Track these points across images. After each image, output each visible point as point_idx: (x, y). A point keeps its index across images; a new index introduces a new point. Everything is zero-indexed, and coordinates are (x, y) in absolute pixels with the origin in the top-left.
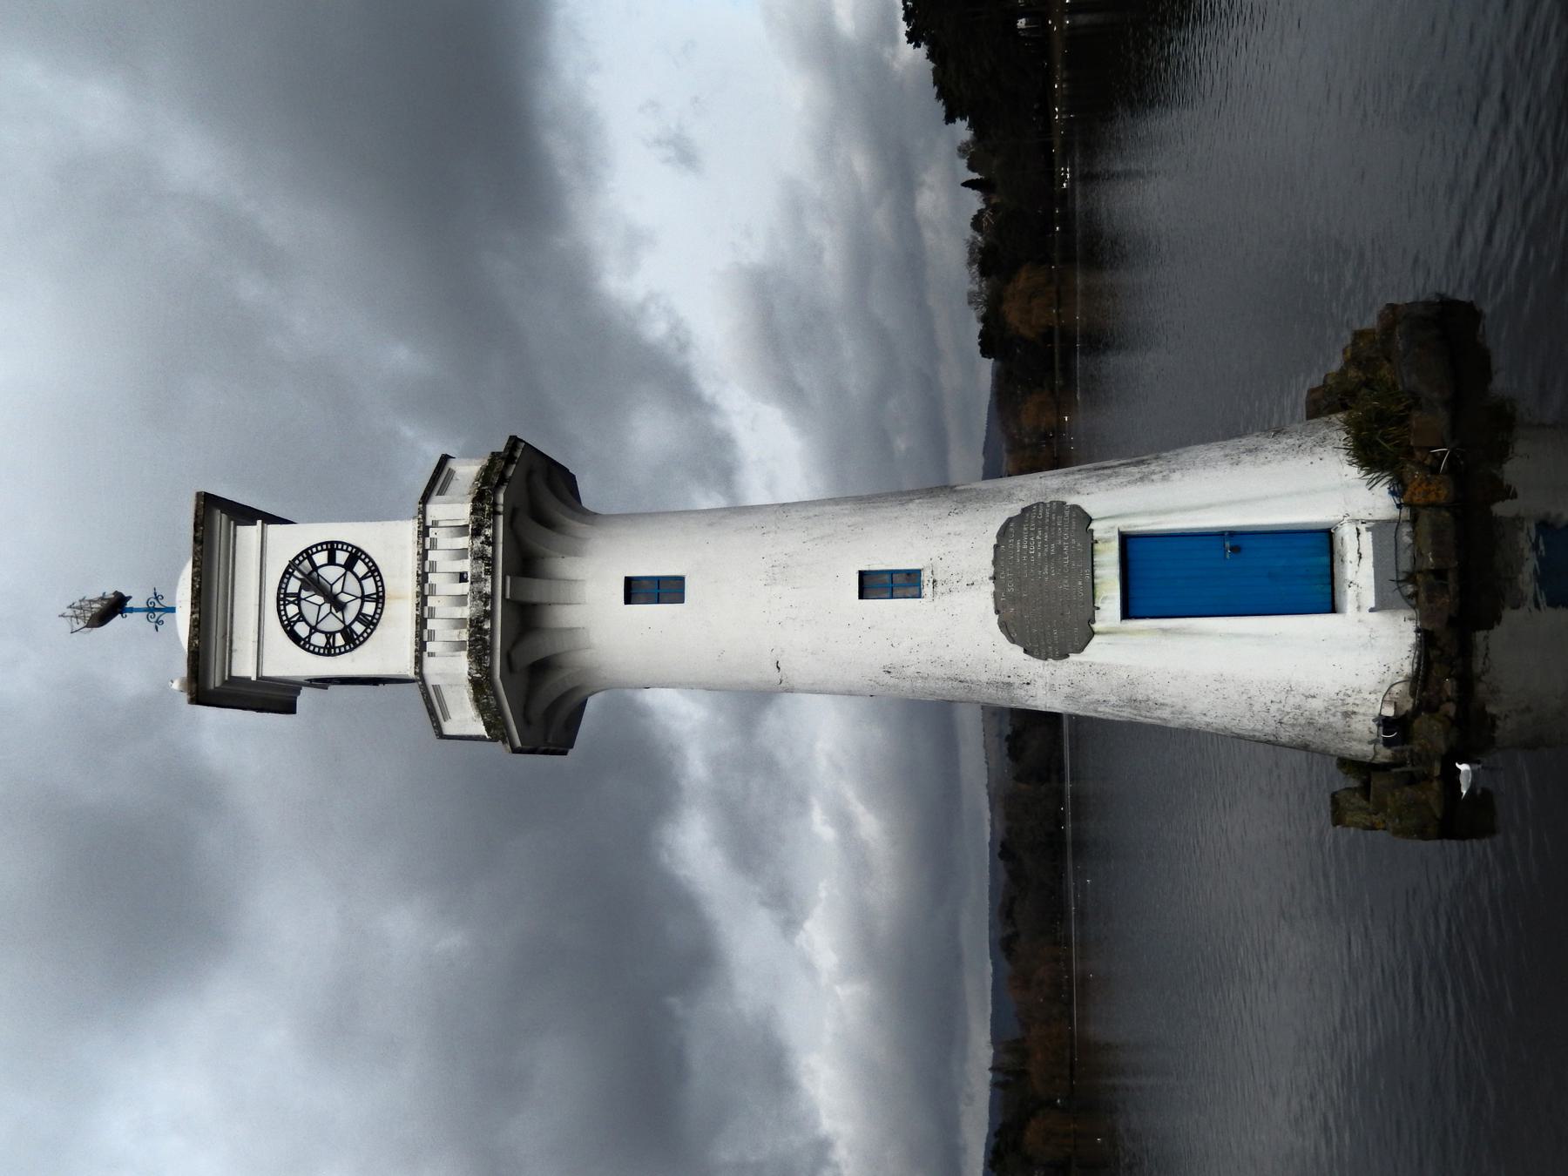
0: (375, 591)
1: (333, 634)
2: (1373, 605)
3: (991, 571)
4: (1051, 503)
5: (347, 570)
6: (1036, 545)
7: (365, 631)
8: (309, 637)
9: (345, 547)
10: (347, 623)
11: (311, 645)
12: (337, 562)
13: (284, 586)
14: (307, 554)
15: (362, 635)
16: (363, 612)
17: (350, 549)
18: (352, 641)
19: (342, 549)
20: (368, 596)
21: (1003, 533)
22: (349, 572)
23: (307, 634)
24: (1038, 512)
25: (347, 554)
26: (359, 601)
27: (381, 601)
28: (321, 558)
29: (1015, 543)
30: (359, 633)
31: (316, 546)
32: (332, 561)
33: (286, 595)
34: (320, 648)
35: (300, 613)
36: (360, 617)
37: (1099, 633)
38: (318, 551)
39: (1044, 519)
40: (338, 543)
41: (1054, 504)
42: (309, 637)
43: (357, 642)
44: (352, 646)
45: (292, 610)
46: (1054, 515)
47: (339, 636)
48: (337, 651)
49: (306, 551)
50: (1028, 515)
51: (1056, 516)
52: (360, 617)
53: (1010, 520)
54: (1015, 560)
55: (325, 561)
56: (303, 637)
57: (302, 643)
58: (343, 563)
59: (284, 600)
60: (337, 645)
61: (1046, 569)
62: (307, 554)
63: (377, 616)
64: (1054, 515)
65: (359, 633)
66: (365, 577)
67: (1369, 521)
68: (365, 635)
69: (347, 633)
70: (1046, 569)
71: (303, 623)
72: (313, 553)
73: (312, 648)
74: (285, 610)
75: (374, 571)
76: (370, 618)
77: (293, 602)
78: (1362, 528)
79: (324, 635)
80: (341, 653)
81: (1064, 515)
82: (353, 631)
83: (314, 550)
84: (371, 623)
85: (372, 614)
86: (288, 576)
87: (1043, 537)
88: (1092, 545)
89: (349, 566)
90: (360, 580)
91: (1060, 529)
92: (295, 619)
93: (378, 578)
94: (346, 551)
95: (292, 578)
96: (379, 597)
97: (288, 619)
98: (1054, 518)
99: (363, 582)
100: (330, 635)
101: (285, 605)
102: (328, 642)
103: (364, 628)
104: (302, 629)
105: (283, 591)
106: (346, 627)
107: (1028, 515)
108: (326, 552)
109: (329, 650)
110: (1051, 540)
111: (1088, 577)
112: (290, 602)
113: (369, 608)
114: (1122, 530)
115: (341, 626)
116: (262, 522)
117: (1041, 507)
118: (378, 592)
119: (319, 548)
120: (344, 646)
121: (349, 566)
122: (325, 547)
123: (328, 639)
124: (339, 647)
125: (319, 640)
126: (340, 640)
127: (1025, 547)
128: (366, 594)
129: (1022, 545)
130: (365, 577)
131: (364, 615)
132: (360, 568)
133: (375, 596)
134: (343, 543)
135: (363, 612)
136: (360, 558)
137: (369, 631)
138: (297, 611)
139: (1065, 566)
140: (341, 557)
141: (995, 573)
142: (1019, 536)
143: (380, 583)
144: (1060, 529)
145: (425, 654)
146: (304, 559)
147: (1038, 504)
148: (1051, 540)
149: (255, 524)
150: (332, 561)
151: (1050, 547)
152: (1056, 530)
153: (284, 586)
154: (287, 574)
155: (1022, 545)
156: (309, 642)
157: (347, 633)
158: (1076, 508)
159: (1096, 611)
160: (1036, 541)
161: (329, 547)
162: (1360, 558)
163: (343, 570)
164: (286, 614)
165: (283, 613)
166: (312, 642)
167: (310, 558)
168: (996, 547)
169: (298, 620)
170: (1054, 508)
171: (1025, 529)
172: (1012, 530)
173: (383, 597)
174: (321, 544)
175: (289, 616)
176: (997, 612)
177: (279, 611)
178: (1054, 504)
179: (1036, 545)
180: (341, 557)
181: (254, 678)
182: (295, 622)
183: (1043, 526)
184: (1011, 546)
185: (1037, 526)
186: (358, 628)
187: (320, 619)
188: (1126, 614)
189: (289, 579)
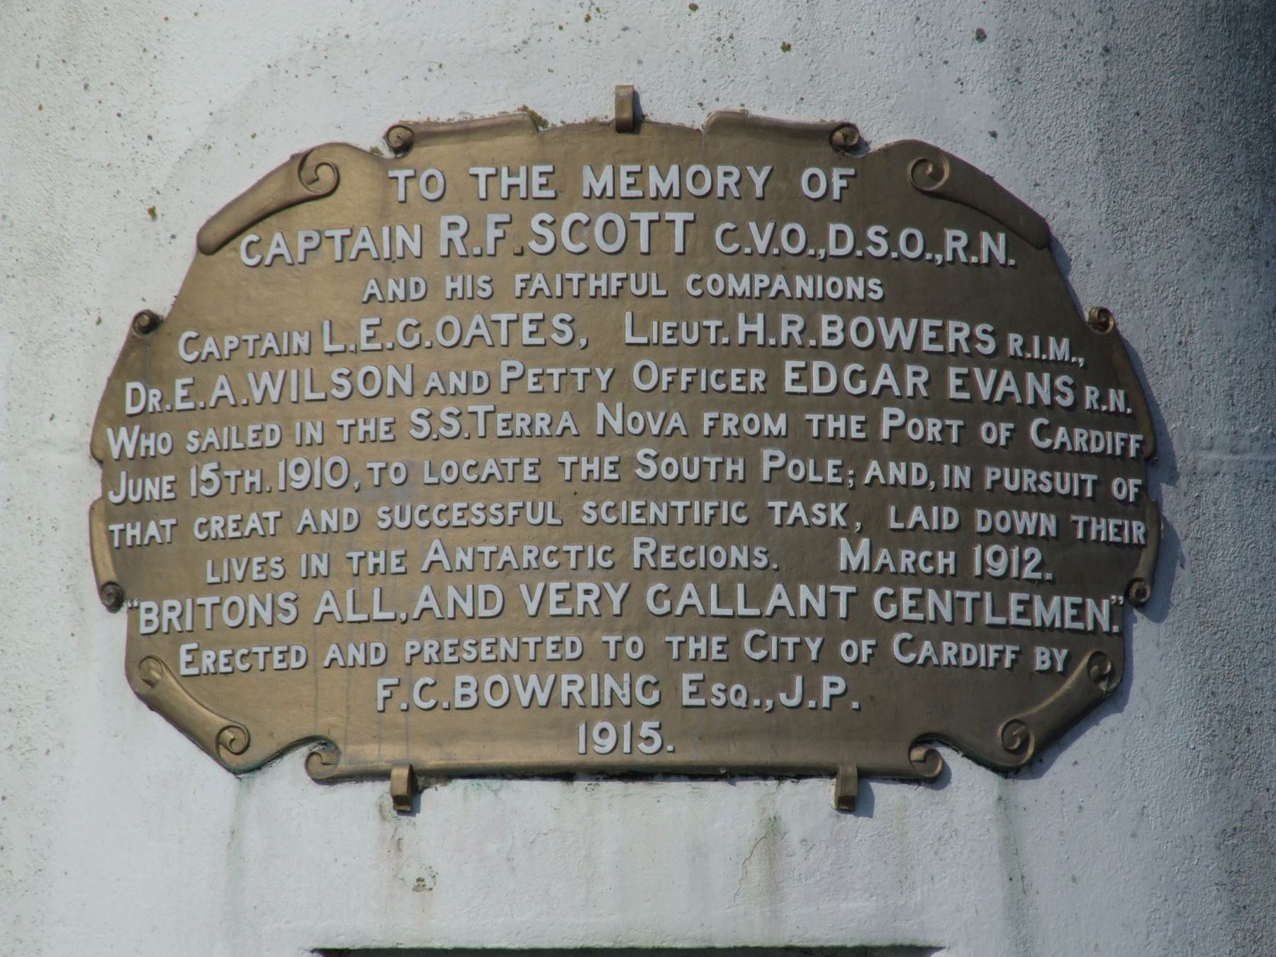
6: (838, 401)
24: (1075, 416)
29: (860, 264)
41: (1137, 530)
46: (1049, 524)
50: (1059, 349)
51: (1034, 539)
61: (671, 465)
87: (900, 447)
98: (1025, 521)
117: (1111, 442)
127: (830, 329)
129: (848, 307)
144: (946, 561)
151: (825, 492)
152: (938, 538)
155: (848, 307)
160: (871, 404)
171: (957, 333)
172: (955, 240)
178: (1137, 530)
185: (975, 410)
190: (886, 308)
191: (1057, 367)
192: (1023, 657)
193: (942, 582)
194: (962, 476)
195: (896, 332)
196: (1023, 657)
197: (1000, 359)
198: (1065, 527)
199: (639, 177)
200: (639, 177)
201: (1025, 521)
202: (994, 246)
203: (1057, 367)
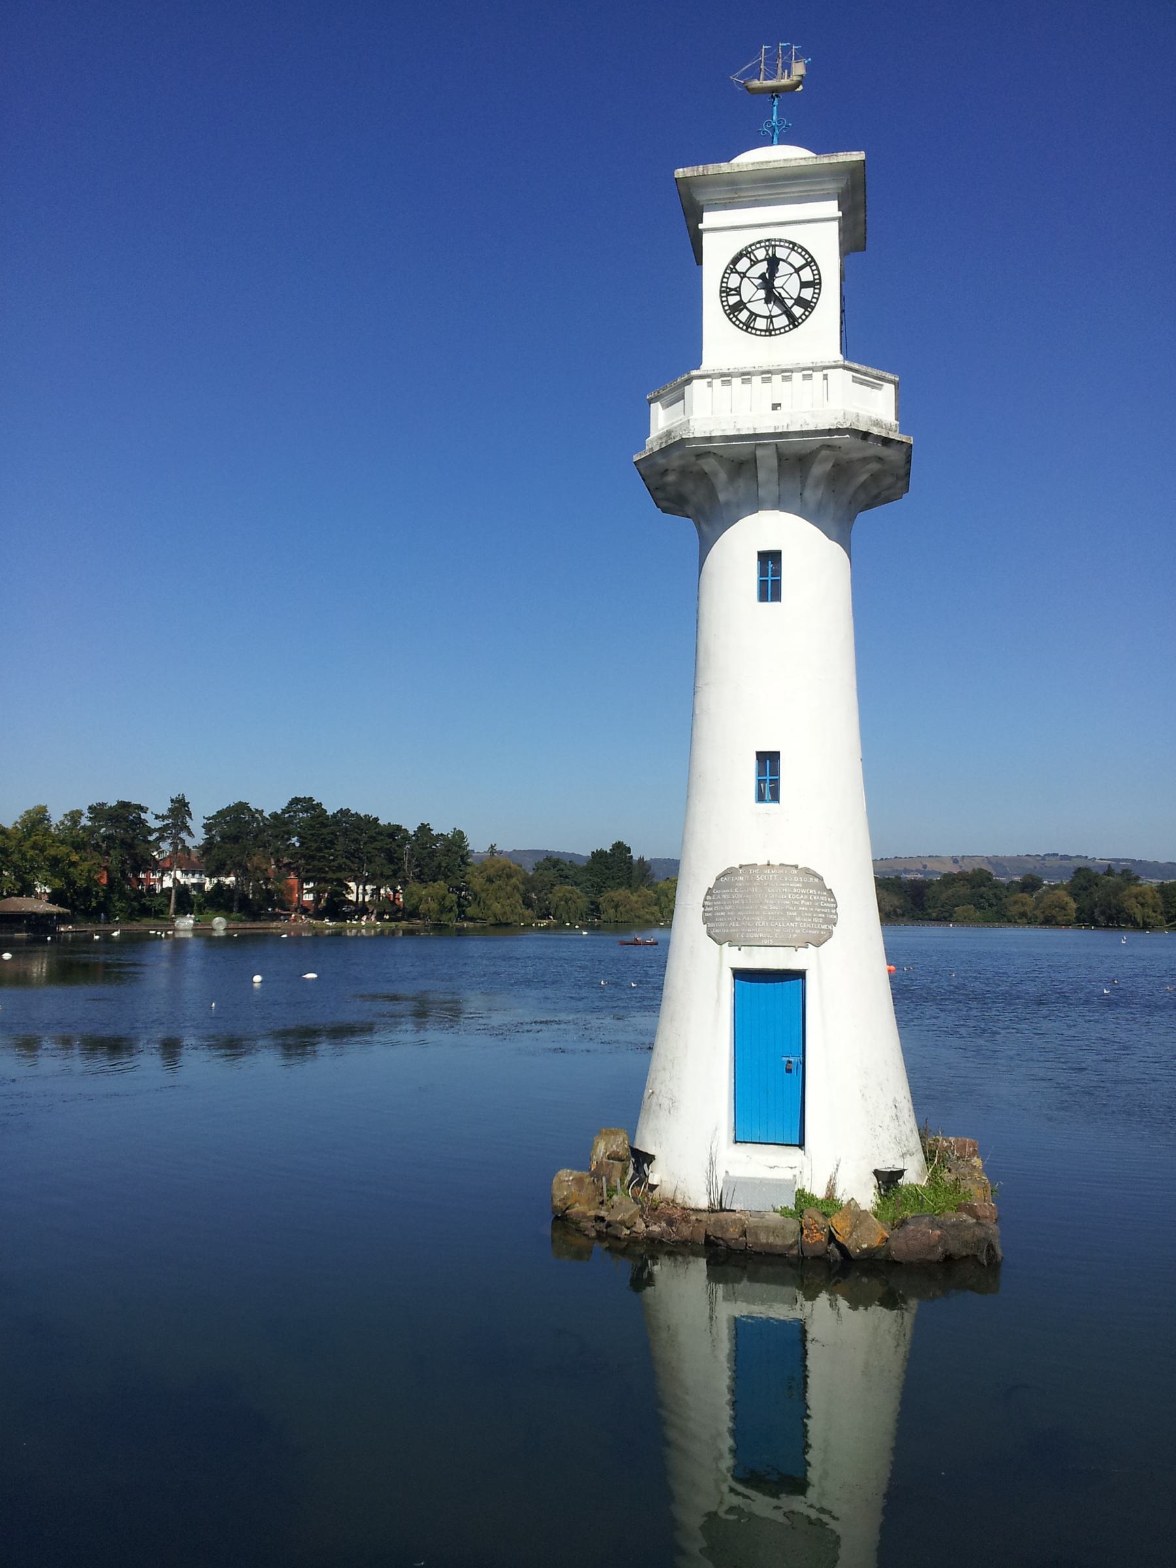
0: (775, 327)
1: (739, 294)
2: (730, 1174)
3: (775, 862)
4: (836, 914)
5: (795, 300)
6: (796, 899)
7: (741, 322)
8: (737, 272)
9: (816, 296)
10: (748, 305)
11: (730, 274)
12: (802, 290)
13: (782, 244)
14: (811, 262)
15: (738, 319)
16: (758, 318)
17: (814, 300)
18: (733, 311)
19: (814, 293)
20: (772, 322)
21: (808, 872)
22: (793, 301)
24: (827, 902)
25: (809, 299)
26: (767, 314)
27: (767, 334)
28: (807, 275)
31: (818, 269)
34: (727, 283)
36: (753, 316)
37: (721, 949)
38: (813, 271)
39: (820, 907)
41: (835, 917)
42: (737, 272)
43: (731, 316)
44: (728, 312)
45: (760, 254)
46: (823, 916)
47: (737, 298)
48: (724, 299)
49: (813, 260)
50: (825, 893)
51: (822, 918)
53: (821, 879)
54: (784, 882)
56: (736, 267)
57: (732, 266)
58: (801, 295)
60: (729, 297)
61: (774, 908)
62: (811, 262)
63: (754, 331)
64: (823, 916)
67: (802, 1178)
68: (737, 323)
69: (740, 306)
70: (774, 908)
71: (749, 265)
72: (811, 267)
73: (727, 275)
74: (761, 247)
76: (752, 325)
77: (767, 254)
78: (796, 1172)
79: (738, 285)
80: (722, 302)
81: (823, 924)
82: (741, 311)
83: (814, 268)
84: (748, 327)
85: (755, 327)
86: (791, 246)
87: (804, 905)
88: (794, 947)
91: (810, 920)
92: (753, 257)
93: (787, 329)
94: (813, 297)
95: (789, 251)
97: (753, 250)
98: (820, 915)
100: (738, 291)
101: (765, 247)
102: (731, 290)
103: (744, 321)
104: (743, 264)
105: (777, 243)
106: (745, 304)
107: (825, 893)
108: (812, 279)
109: (725, 291)
110: (800, 913)
111: (766, 942)
112: (767, 251)
113: (761, 324)
114: (807, 972)
115: (745, 301)
116: (839, 219)
117: (832, 905)
118: (775, 330)
119: (816, 272)
120: (728, 305)
122: (817, 277)
123: (735, 290)
124: (727, 301)
125: (734, 280)
126: (733, 300)
127: (795, 890)
128: (774, 319)
131: (755, 320)
133: (771, 328)
135: (758, 318)
136: (806, 310)
137: (741, 325)
138: (759, 259)
139: (776, 924)
141: (773, 866)
142: (806, 885)
144: (810, 920)
145: (710, 380)
146: (806, 260)
147: (835, 902)
148: (800, 913)
149: (839, 210)
150: (804, 285)
151: (794, 911)
152: (809, 917)
153: (782, 244)
154: (793, 246)
155: (797, 888)
156: (732, 272)
157: (740, 306)
158: (830, 934)
159: (737, 947)
160: (800, 900)
161: (816, 281)
162: (771, 1168)
164: (757, 248)
165: (758, 246)
166: (732, 275)
167: (807, 264)
168: (796, 867)
169: (751, 260)
170: (831, 916)
171: (811, 891)
172: (811, 879)
173: (771, 335)
174: (819, 274)
175: (755, 252)
176: (741, 867)
178: (835, 917)
179: (796, 899)
181: (701, 226)
182: (750, 258)
183: (814, 906)
184: (796, 879)
185: (814, 901)
186: (744, 316)
187: (752, 279)
188: (740, 975)
189: (788, 248)
190: (802, 888)
191: (824, 896)
192: (820, 932)
193: (809, 922)
194: (812, 909)
195: (803, 891)
196: (820, 932)
197: (817, 895)
198: (826, 916)
199: (770, 871)
200: (770, 871)
201: (820, 915)
202: (816, 880)
203: (824, 896)
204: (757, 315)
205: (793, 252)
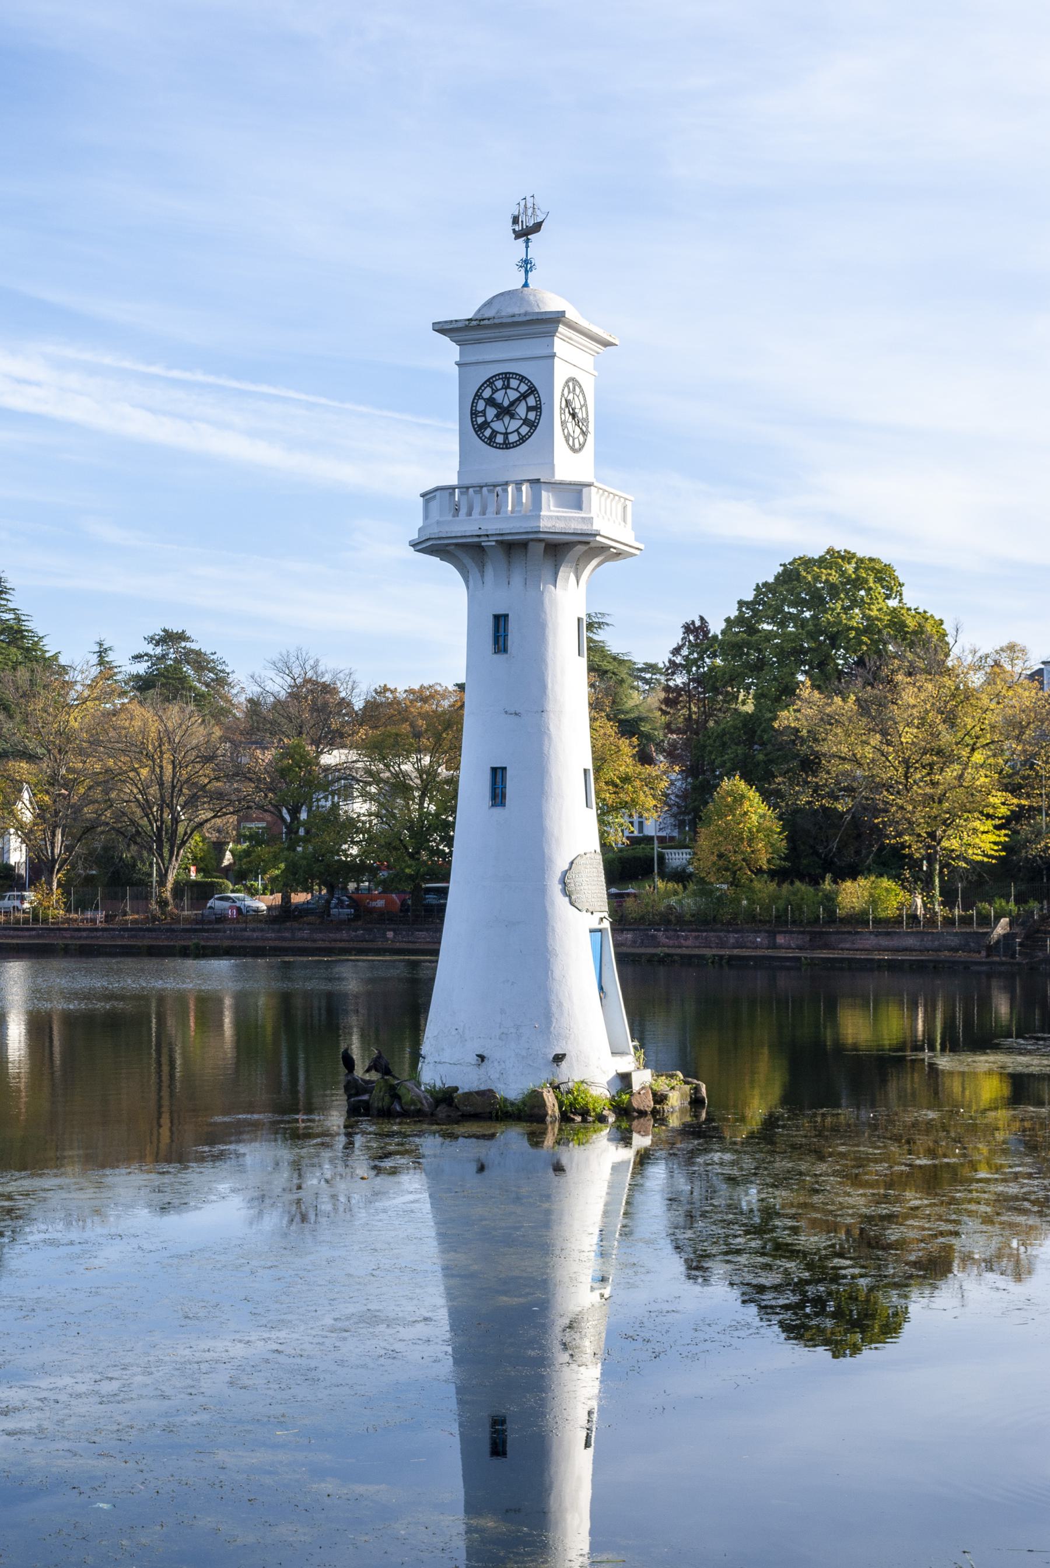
1: (485, 415)
8: (483, 398)
20: (507, 438)
23: (485, 397)
30: (485, 434)
32: (529, 409)
33: (509, 379)
35: (498, 390)
40: (541, 412)
42: (483, 398)
52: (494, 433)
55: (529, 405)
59: (506, 377)
65: (485, 434)
66: (519, 434)
69: (486, 425)
75: (523, 439)
77: (504, 384)
82: (486, 429)
89: (526, 422)
90: (517, 430)
96: (506, 445)
99: (516, 433)
102: (479, 412)
112: (504, 382)
118: (510, 444)
121: (526, 422)
123: (481, 412)
126: (480, 420)
130: (519, 434)
131: (495, 436)
132: (524, 430)
134: (540, 416)
140: (532, 416)
143: (515, 445)
150: (529, 409)
154: (522, 379)
157: (486, 425)
163: (523, 418)
169: (493, 389)
177: (498, 375)
180: (532, 416)
186: (488, 433)
204: (498, 432)
205: (522, 384)
